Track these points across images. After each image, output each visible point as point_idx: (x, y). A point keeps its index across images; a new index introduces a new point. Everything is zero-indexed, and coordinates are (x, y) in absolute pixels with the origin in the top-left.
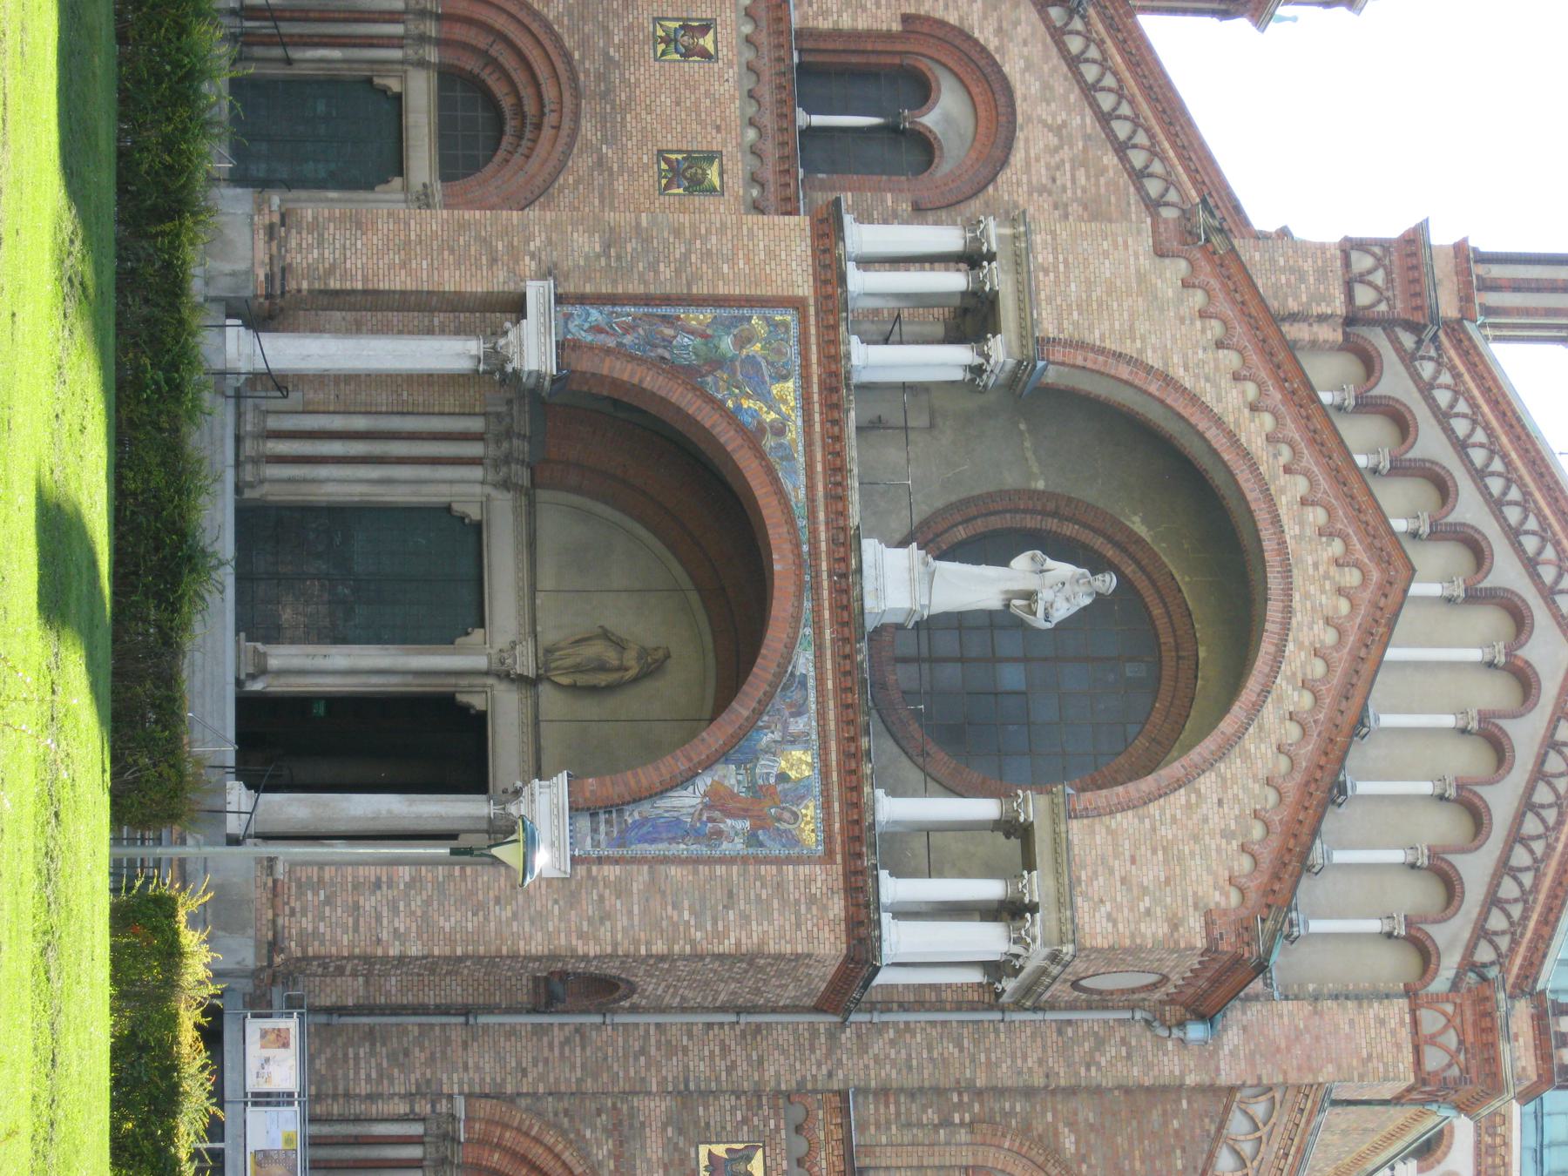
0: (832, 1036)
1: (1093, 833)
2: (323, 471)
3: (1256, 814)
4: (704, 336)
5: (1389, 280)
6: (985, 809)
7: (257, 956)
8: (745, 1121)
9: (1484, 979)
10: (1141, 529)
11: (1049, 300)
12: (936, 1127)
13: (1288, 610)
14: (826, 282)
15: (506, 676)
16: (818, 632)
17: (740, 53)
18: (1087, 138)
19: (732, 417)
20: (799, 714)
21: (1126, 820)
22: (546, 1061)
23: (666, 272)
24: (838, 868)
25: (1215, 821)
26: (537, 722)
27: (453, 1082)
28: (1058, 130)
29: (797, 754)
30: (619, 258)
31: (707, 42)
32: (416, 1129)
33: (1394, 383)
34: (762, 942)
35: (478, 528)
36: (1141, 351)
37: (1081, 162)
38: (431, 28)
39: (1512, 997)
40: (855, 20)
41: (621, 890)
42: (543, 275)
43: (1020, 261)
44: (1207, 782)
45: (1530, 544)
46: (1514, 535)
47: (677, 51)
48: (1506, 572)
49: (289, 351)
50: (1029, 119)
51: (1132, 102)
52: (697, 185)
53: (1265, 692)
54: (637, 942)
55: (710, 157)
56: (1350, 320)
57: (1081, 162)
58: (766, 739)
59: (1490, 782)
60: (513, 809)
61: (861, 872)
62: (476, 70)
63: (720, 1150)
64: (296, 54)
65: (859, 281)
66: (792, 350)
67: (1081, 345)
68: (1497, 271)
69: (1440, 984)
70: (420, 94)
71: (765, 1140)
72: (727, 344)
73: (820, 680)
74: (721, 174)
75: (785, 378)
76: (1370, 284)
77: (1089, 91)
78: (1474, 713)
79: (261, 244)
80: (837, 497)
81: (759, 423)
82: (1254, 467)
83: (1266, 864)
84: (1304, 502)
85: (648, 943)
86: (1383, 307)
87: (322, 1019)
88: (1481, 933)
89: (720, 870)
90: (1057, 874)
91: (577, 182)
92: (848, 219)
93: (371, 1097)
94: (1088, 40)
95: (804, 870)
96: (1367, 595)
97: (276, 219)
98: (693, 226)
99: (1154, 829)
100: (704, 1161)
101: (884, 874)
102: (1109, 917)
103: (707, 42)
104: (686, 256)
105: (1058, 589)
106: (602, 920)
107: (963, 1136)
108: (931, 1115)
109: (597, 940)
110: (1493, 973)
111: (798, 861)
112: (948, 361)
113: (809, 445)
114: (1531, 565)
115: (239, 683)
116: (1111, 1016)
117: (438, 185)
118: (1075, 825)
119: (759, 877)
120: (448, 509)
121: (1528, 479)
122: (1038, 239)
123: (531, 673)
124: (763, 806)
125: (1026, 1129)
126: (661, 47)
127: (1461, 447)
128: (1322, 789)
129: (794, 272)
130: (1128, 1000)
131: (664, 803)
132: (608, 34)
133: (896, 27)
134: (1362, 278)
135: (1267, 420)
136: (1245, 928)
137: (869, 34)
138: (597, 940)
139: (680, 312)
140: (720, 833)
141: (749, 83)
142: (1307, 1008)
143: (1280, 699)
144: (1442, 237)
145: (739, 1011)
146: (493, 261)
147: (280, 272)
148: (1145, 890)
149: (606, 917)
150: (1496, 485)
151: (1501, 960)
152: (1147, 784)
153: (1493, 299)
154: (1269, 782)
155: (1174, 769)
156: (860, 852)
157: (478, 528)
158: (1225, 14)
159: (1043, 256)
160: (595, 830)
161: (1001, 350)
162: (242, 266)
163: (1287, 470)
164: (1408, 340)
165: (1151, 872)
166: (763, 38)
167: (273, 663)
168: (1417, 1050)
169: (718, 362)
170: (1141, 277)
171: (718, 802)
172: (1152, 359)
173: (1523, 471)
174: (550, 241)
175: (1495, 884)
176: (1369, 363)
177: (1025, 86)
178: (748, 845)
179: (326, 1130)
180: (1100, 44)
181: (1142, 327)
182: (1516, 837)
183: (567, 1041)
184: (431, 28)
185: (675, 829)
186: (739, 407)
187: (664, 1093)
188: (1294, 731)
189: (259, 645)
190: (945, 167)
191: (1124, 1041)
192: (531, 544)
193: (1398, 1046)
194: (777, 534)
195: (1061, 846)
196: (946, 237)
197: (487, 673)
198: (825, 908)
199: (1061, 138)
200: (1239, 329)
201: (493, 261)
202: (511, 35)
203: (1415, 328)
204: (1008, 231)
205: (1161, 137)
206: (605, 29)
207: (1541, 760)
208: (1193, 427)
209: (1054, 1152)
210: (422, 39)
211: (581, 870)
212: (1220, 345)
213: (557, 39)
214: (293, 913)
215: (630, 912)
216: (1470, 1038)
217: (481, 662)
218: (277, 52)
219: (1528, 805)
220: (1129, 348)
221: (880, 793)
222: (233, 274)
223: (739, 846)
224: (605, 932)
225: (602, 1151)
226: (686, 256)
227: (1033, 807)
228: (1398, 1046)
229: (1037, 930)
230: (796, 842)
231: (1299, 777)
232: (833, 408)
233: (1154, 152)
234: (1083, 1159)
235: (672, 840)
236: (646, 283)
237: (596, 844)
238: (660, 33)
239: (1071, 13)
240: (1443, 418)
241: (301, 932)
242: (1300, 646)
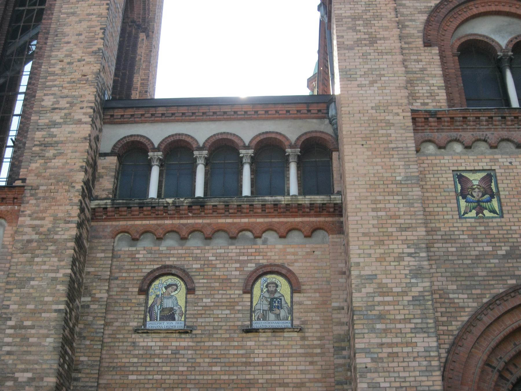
17: (483, 153)
31: (475, 179)
40: (435, 76)
47: (490, 201)
62: (510, 386)
103: (475, 179)
126: (486, 213)
132: (480, 257)
133: (435, 50)
166: (468, 136)
202: (493, 344)
206: (478, 257)
238: (473, 213)
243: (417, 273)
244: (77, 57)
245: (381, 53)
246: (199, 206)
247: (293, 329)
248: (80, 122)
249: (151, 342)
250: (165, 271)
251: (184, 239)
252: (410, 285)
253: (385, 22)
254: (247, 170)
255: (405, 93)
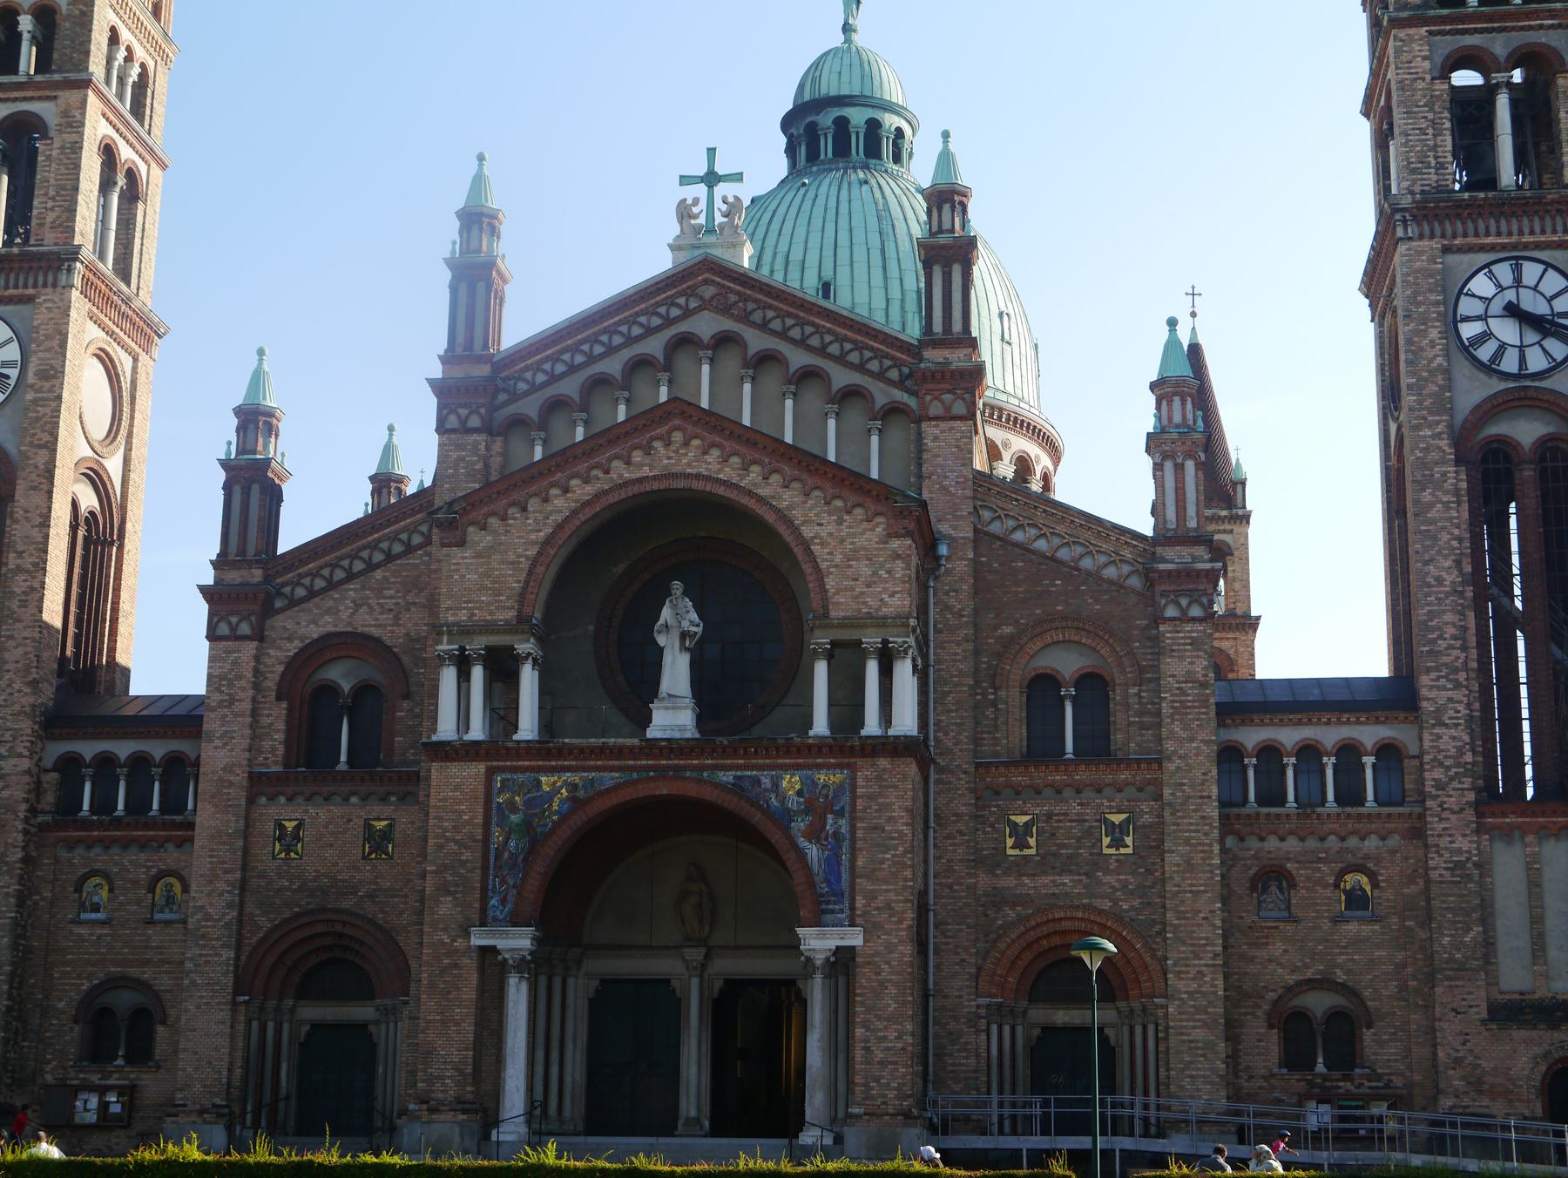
0: (941, 770)
1: (838, 603)
2: (568, 1079)
3: (828, 503)
4: (510, 832)
5: (464, 406)
6: (821, 670)
7: (915, 1126)
8: (992, 826)
9: (910, 376)
10: (622, 567)
11: (491, 613)
12: (997, 709)
13: (698, 476)
14: (477, 754)
15: (704, 967)
16: (706, 768)
18: (363, 588)
19: (564, 817)
20: (759, 782)
21: (830, 583)
22: (956, 947)
23: (466, 855)
24: (860, 762)
25: (832, 528)
26: (736, 948)
27: (970, 1004)
28: (357, 606)
29: (785, 784)
30: (456, 885)
31: (290, 825)
32: (994, 1028)
33: (530, 407)
34: (906, 809)
35: (603, 981)
36: (527, 558)
37: (379, 593)
38: (271, 1004)
39: (921, 360)
41: (871, 896)
42: (467, 935)
43: (466, 631)
44: (807, 532)
45: (636, 331)
46: (630, 341)
48: (654, 347)
49: (514, 1099)
50: (350, 624)
51: (341, 558)
52: (387, 835)
53: (750, 493)
54: (905, 888)
55: (368, 826)
56: (488, 429)
57: (379, 593)
58: (774, 801)
59: (787, 364)
60: (818, 963)
61: (863, 747)
63: (1010, 842)
64: (283, 1092)
65: (477, 732)
66: (521, 777)
67: (522, 596)
68: (460, 339)
69: (912, 402)
70: (312, 1012)
71: (1004, 816)
72: (515, 818)
73: (738, 768)
74: (379, 819)
75: (539, 783)
76: (467, 417)
77: (332, 585)
78: (743, 372)
79: (442, 1117)
80: (618, 752)
81: (568, 798)
82: (605, 493)
83: (860, 500)
84: (628, 463)
85: (906, 880)
86: (483, 411)
87: (930, 1086)
88: (880, 376)
89: (859, 834)
90: (865, 626)
91: (382, 911)
92: (434, 738)
93: (978, 1056)
94: (298, 584)
95: (860, 782)
96: (690, 428)
97: (425, 1107)
98: (437, 837)
99: (836, 566)
100: (1017, 852)
101: (863, 733)
102: (892, 595)
103: (290, 825)
104: (456, 842)
105: (677, 620)
106: (891, 908)
107: (1002, 693)
108: (989, 712)
109: (904, 912)
110: (906, 370)
111: (854, 786)
112: (529, 678)
113: (585, 769)
114: (650, 331)
115: (705, 1136)
116: (932, 601)
117: (378, 1002)
118: (833, 614)
119: (865, 808)
120: (590, 1000)
121: (595, 329)
122: (451, 619)
123: (704, 950)
124: (817, 805)
125: (999, 656)
127: (573, 369)
128: (804, 462)
129: (474, 772)
130: (923, 588)
131: (815, 867)
133: (284, 705)
134: (463, 422)
135: (574, 482)
136: (901, 514)
137: (288, 722)
138: (904, 912)
139: (493, 847)
140: (836, 834)
141: (319, 799)
142: (926, 483)
143: (755, 485)
144: (437, 372)
145: (926, 827)
146: (456, 966)
147: (460, 1105)
148: (875, 574)
149: (888, 906)
150: (598, 349)
151: (897, 364)
152: (807, 568)
153: (478, 343)
154: (807, 495)
155: (798, 550)
156: (846, 742)
157: (603, 981)
158: (280, 499)
159: (463, 616)
160: (833, 912)
161: (526, 646)
162: (457, 1130)
163: (607, 472)
164: (503, 397)
165: (865, 570)
167: (693, 1113)
168: (953, 418)
169: (527, 827)
170: (478, 555)
171: (815, 834)
172: (532, 552)
173: (590, 332)
174: (445, 930)
175: (851, 366)
176: (519, 422)
177: (328, 625)
178: (843, 816)
179: (995, 1085)
180: (301, 576)
181: (511, 557)
182: (822, 351)
183: (944, 934)
184: (271, 1004)
185: (833, 863)
186: (557, 812)
187: (975, 876)
188: (775, 478)
189: (680, 1123)
190: (378, 678)
191: (947, 593)
192: (619, 948)
193: (951, 429)
194: (643, 791)
195: (846, 623)
196: (449, 676)
197: (701, 978)
198: (884, 770)
199: (361, 605)
200: (515, 497)
201: (456, 966)
203: (497, 391)
204: (445, 638)
205: (364, 541)
206: (279, 890)
207: (773, 333)
208: (578, 528)
209: (1012, 637)
210: (278, 1010)
211: (859, 920)
212: (524, 509)
213: (286, 921)
214: (885, 1103)
215: (887, 891)
216: (947, 386)
217: (695, 981)
218: (281, 1105)
219: (802, 343)
220: (525, 565)
221: (811, 733)
222: (462, 1135)
223: (844, 823)
224: (899, 907)
225: (1012, 914)
226: (456, 842)
227: (822, 640)
228: (951, 429)
229: (900, 640)
230: (841, 786)
231: (805, 476)
232: (562, 752)
233: (374, 547)
234: (1017, 621)
235: (839, 864)
236: (473, 870)
237: (842, 911)
239: (280, 594)
240: (553, 379)
241: (898, 1097)
242: (720, 471)
243: (230, 905)
244: (16, 687)
245: (236, 715)
246: (117, 823)
247: (178, 922)
248: (21, 756)
249: (83, 931)
250: (94, 873)
251: (107, 848)
252: (225, 914)
253: (243, 683)
254: (157, 785)
255: (247, 755)
